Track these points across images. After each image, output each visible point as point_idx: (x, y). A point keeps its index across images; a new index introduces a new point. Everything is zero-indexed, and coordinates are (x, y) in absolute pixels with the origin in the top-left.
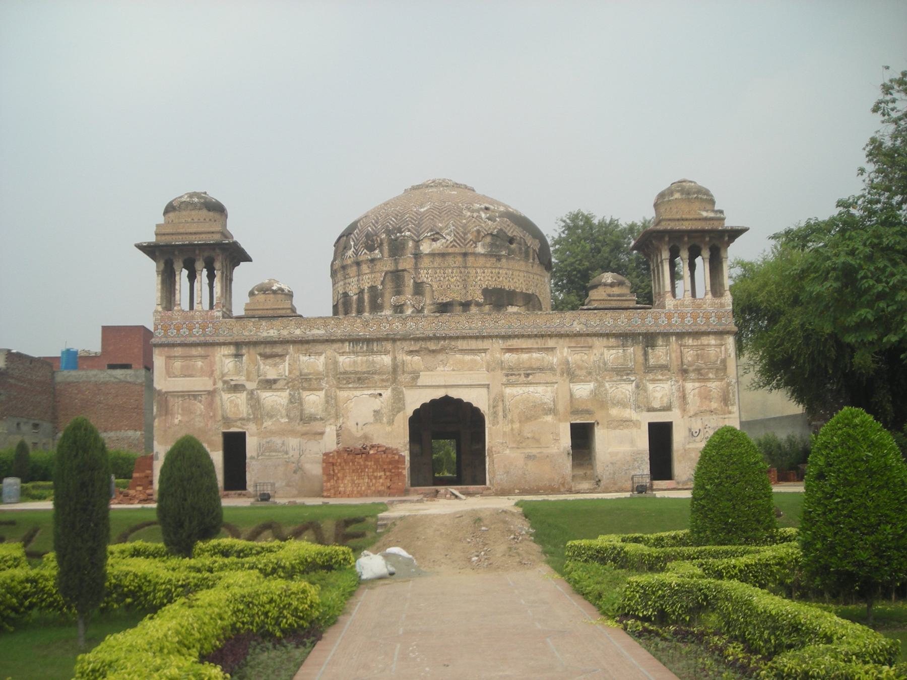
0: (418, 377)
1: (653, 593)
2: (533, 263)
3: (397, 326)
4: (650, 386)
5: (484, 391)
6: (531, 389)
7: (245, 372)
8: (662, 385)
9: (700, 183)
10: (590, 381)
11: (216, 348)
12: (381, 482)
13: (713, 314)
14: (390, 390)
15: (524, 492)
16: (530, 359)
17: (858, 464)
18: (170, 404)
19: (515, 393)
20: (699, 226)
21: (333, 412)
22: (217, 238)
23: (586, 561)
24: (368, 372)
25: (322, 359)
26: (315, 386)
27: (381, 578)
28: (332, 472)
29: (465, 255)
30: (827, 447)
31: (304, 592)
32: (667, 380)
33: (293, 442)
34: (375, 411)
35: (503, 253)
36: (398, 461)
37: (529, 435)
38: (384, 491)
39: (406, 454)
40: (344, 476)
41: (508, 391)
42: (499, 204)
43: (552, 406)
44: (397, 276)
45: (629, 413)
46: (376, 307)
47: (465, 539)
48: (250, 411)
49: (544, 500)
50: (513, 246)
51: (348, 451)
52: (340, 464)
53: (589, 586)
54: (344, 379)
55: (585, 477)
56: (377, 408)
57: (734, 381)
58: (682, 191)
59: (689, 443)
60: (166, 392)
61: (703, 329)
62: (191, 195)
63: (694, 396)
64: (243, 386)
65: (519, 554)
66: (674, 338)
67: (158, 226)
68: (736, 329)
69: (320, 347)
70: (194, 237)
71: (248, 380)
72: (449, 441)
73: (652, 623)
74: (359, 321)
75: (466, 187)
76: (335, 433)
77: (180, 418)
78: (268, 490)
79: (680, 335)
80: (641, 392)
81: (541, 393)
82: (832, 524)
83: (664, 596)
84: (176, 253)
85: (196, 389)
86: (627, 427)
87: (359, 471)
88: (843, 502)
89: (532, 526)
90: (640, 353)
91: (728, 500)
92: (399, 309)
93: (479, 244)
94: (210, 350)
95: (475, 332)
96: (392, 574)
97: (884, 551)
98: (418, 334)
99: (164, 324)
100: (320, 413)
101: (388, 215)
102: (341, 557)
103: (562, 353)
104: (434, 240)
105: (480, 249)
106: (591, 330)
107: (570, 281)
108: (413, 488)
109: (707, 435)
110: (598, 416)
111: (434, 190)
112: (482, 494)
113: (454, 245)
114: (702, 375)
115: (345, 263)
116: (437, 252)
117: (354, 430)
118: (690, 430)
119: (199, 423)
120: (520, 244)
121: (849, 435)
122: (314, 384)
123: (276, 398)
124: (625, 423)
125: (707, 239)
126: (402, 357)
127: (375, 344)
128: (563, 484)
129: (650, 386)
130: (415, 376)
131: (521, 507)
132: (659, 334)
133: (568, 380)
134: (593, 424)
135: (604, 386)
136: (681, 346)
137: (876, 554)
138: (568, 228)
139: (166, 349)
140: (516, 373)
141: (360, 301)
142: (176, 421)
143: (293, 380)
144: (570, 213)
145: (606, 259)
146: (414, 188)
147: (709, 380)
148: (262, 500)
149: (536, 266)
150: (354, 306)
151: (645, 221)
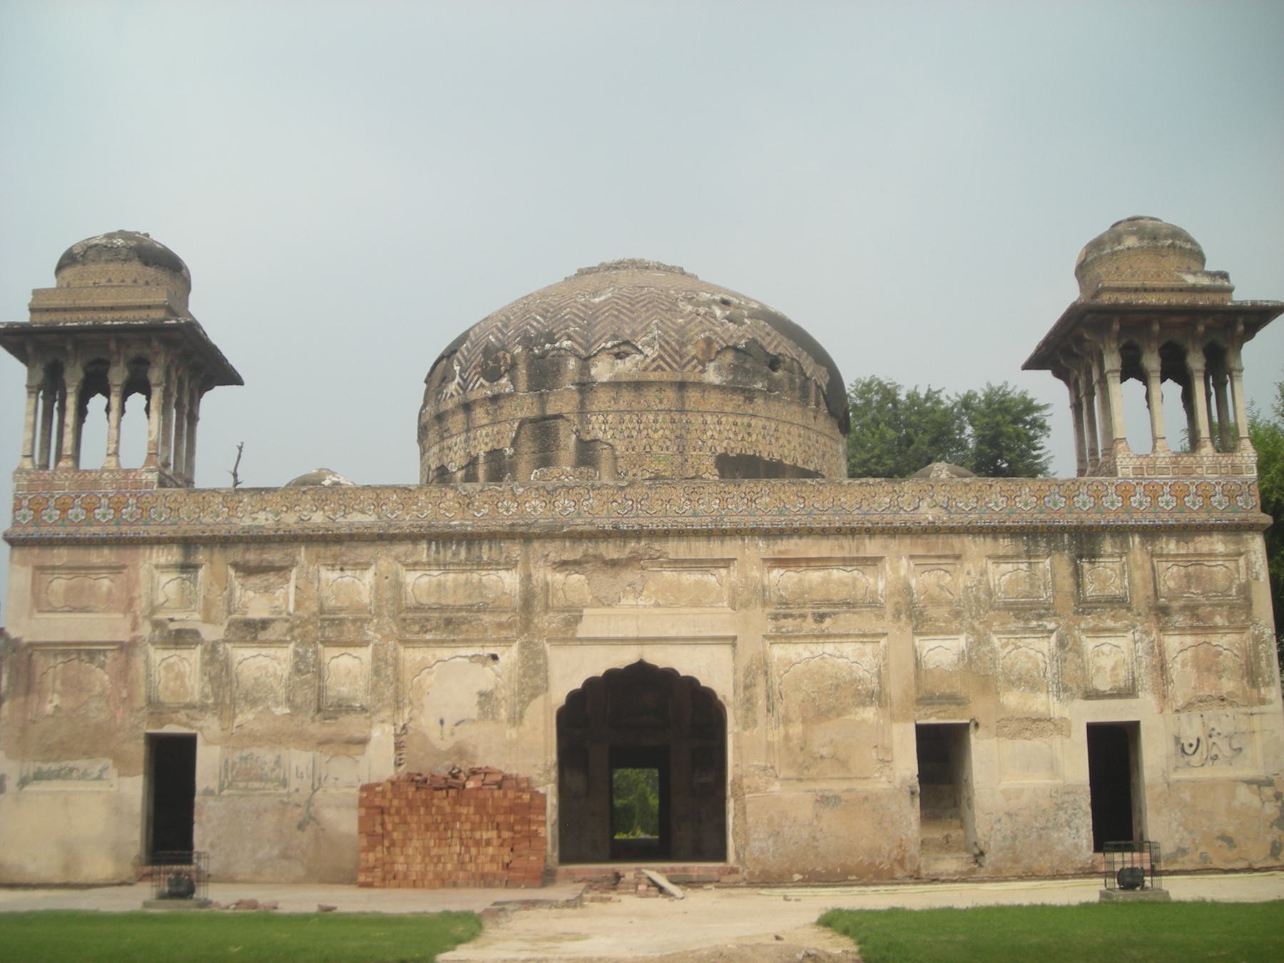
0: (578, 619)
2: (816, 412)
3: (537, 509)
4: (1089, 644)
5: (724, 652)
7: (201, 604)
8: (1114, 641)
10: (958, 632)
11: (141, 551)
12: (489, 857)
13: (1218, 488)
14: (515, 647)
15: (815, 879)
16: (826, 582)
18: (38, 673)
19: (794, 658)
20: (1186, 300)
21: (389, 693)
22: (157, 315)
24: (469, 608)
25: (369, 577)
26: (352, 636)
28: (379, 829)
29: (682, 386)
32: (1126, 629)
33: (299, 759)
34: (481, 694)
35: (759, 386)
36: (529, 807)
37: (824, 751)
38: (494, 876)
40: (407, 839)
41: (778, 652)
42: (748, 300)
43: (874, 685)
44: (543, 430)
45: (1043, 703)
48: (208, 690)
49: (893, 912)
50: (778, 374)
51: (419, 782)
52: (398, 812)
54: (414, 621)
55: (947, 845)
58: (1141, 233)
59: (1176, 768)
60: (31, 645)
61: (1200, 518)
62: (110, 236)
63: (1184, 665)
64: (195, 633)
66: (1137, 539)
67: (36, 293)
68: (1268, 519)
69: (365, 552)
71: (207, 619)
74: (451, 495)
76: (392, 740)
77: (57, 700)
79: (1151, 532)
80: (1070, 656)
81: (850, 657)
84: (69, 347)
86: (1041, 733)
87: (442, 827)
90: (1065, 569)
93: (711, 367)
94: (127, 555)
98: (581, 524)
100: (360, 694)
103: (895, 570)
104: (618, 356)
106: (957, 520)
109: (1214, 751)
110: (978, 709)
112: (718, 883)
113: (659, 367)
114: (1198, 618)
115: (443, 408)
116: (624, 379)
117: (434, 734)
118: (1177, 740)
119: (97, 712)
120: (790, 370)
122: (350, 631)
123: (266, 661)
124: (1035, 724)
125: (1201, 328)
126: (544, 575)
127: (485, 547)
128: (901, 862)
129: (1089, 644)
130: (573, 616)
131: (846, 932)
132: (1105, 529)
133: (909, 630)
134: (966, 726)
135: (988, 642)
136: (1152, 556)
139: (36, 551)
140: (795, 612)
142: (49, 708)
143: (304, 622)
146: (582, 273)
147: (1214, 629)
148: (172, 895)
151: (992, 389)
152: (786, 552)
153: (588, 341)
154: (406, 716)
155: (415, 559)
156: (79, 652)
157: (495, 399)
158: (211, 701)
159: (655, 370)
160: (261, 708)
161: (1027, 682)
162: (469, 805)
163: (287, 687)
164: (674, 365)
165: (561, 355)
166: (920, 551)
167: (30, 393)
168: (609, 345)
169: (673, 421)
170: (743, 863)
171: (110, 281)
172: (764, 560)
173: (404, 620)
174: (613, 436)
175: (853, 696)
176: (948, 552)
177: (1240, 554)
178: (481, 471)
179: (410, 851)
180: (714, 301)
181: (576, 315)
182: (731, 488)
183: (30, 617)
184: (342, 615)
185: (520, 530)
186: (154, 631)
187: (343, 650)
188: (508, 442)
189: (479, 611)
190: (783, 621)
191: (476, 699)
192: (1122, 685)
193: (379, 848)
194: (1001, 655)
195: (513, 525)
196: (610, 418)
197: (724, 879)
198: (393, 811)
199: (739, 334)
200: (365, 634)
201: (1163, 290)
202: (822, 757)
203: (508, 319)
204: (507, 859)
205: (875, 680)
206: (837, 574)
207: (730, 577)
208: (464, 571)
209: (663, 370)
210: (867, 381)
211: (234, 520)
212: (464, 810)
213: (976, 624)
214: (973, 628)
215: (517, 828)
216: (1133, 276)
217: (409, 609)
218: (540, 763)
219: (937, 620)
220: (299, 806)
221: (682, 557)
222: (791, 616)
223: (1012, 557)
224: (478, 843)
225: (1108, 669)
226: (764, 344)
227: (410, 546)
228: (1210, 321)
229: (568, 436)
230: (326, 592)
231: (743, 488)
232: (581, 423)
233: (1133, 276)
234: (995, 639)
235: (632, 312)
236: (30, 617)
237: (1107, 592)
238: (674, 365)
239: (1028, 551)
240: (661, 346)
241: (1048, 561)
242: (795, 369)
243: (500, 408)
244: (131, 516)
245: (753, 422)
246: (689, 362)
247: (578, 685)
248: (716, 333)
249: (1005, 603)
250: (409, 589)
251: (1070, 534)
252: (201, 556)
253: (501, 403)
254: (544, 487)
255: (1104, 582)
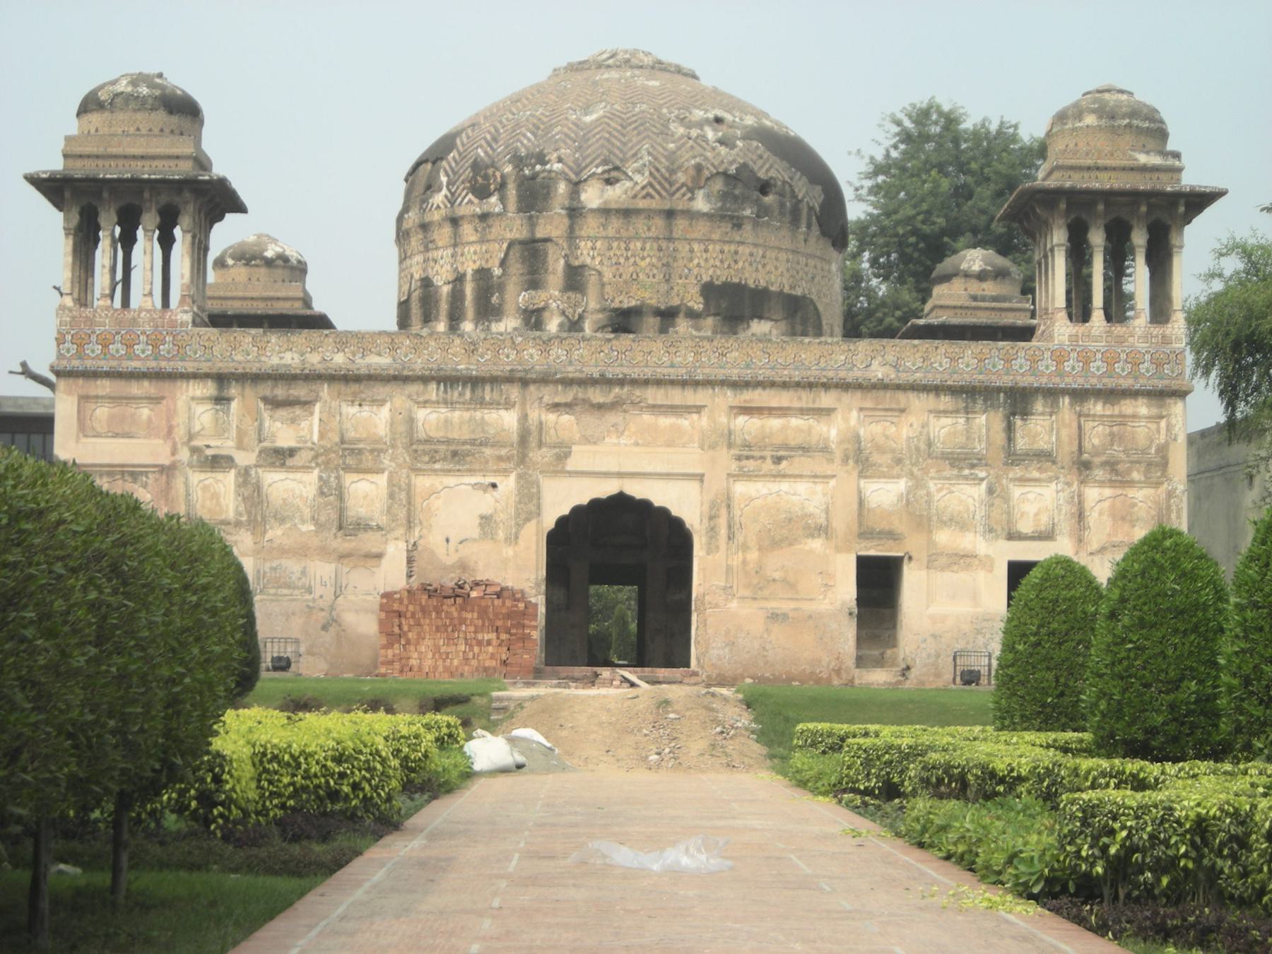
0: (567, 455)
1: (879, 758)
3: (532, 357)
4: (1016, 492)
5: (693, 486)
6: (786, 486)
7: (234, 433)
8: (1038, 490)
9: (1139, 97)
10: (899, 477)
11: (179, 383)
12: (490, 654)
13: (1147, 357)
14: (513, 477)
16: (784, 428)
17: (1160, 600)
19: (754, 494)
21: (402, 514)
23: (824, 752)
24: (472, 442)
25: (385, 412)
26: (370, 465)
27: (504, 771)
28: (396, 630)
29: (670, 214)
30: (1124, 577)
31: (417, 737)
32: (1050, 480)
33: (322, 571)
34: (482, 517)
35: (748, 212)
36: (524, 614)
37: (777, 575)
38: (495, 669)
39: (540, 601)
40: (420, 638)
41: (740, 488)
42: (744, 108)
43: (822, 521)
44: (531, 252)
46: (488, 311)
47: (639, 730)
48: (242, 508)
50: (769, 199)
51: (430, 591)
52: (413, 615)
53: (811, 769)
54: (425, 453)
56: (487, 511)
57: (1181, 487)
61: (1126, 383)
63: (1101, 514)
65: (727, 755)
66: (1067, 400)
67: (68, 139)
69: (381, 390)
70: (140, 164)
71: (240, 446)
72: (620, 581)
73: (876, 797)
74: (458, 341)
75: (679, 71)
76: (405, 554)
78: (289, 651)
79: (1080, 395)
80: (997, 501)
81: (802, 494)
82: (1122, 678)
83: (891, 762)
85: (136, 462)
86: (968, 567)
87: (450, 629)
88: (1137, 648)
89: (756, 720)
90: (998, 423)
91: (1048, 669)
92: (533, 319)
93: (700, 194)
94: (166, 386)
95: (681, 373)
96: (520, 767)
97: (1185, 716)
98: (571, 371)
99: (73, 334)
101: (518, 125)
102: (445, 730)
103: (846, 420)
104: (609, 182)
105: (701, 204)
106: (904, 378)
107: (905, 258)
108: (549, 668)
110: (909, 544)
111: (614, 74)
113: (648, 195)
114: (1117, 473)
115: (427, 219)
116: (613, 206)
120: (782, 195)
121: (1154, 561)
122: (368, 460)
124: (963, 559)
125: (1144, 209)
127: (488, 388)
128: (838, 672)
129: (1016, 492)
130: (563, 454)
132: (1037, 390)
133: (855, 474)
136: (1080, 416)
137: (1175, 720)
138: (906, 137)
139: (80, 381)
140: (757, 454)
141: (457, 297)
143: (327, 451)
144: (914, 106)
145: (983, 212)
147: (1131, 483)
149: (812, 240)
150: (444, 306)
152: (751, 401)
153: (579, 166)
154: (417, 534)
155: (426, 397)
156: (123, 473)
157: (484, 217)
158: (244, 518)
159: (644, 197)
160: (288, 525)
161: (957, 523)
162: (473, 611)
163: (312, 507)
164: (664, 193)
165: (551, 180)
166: (869, 404)
167: (67, 235)
168: (600, 170)
169: (660, 249)
170: (703, 668)
171: (138, 129)
172: (732, 408)
173: (416, 451)
174: (601, 263)
175: (804, 528)
176: (894, 406)
177: (1162, 417)
178: (469, 289)
179: (423, 649)
180: (707, 121)
181: (567, 135)
182: (705, 343)
183: (78, 440)
184: (361, 446)
185: (519, 375)
186: (191, 456)
187: (362, 476)
188: (497, 263)
189: (481, 444)
190: (745, 462)
191: (478, 521)
192: (1043, 528)
193: (396, 646)
194: (936, 498)
195: (512, 371)
196: (598, 244)
197: (686, 680)
198: (409, 615)
199: (728, 158)
200: (381, 462)
201: (1114, 169)
202: (774, 580)
203: (497, 130)
204: (504, 657)
205: (823, 515)
206: (795, 422)
207: (703, 421)
208: (468, 410)
209: (652, 197)
210: (924, 105)
211: (263, 359)
212: (469, 616)
213: (915, 470)
214: (912, 474)
215: (513, 631)
216: (1087, 154)
217: (419, 442)
218: (533, 577)
219: (881, 465)
220: (322, 610)
221: (659, 402)
222: (753, 457)
223: (951, 412)
224: (480, 643)
225: (1031, 514)
226: (756, 168)
227: (422, 387)
228: (1153, 200)
229: (557, 260)
230: (347, 425)
231: (715, 343)
232: (570, 248)
233: (1087, 154)
234: (932, 486)
235: (624, 135)
236: (78, 440)
237: (1035, 447)
238: (664, 193)
239: (966, 407)
240: (651, 174)
241: (984, 417)
242: (787, 192)
243: (490, 227)
244: (168, 352)
245: (741, 249)
246: (678, 189)
247: (566, 511)
248: (706, 159)
249: (943, 453)
250: (420, 424)
251: (1005, 393)
252: (233, 390)
253: (490, 221)
254: (540, 338)
255: (1034, 437)
